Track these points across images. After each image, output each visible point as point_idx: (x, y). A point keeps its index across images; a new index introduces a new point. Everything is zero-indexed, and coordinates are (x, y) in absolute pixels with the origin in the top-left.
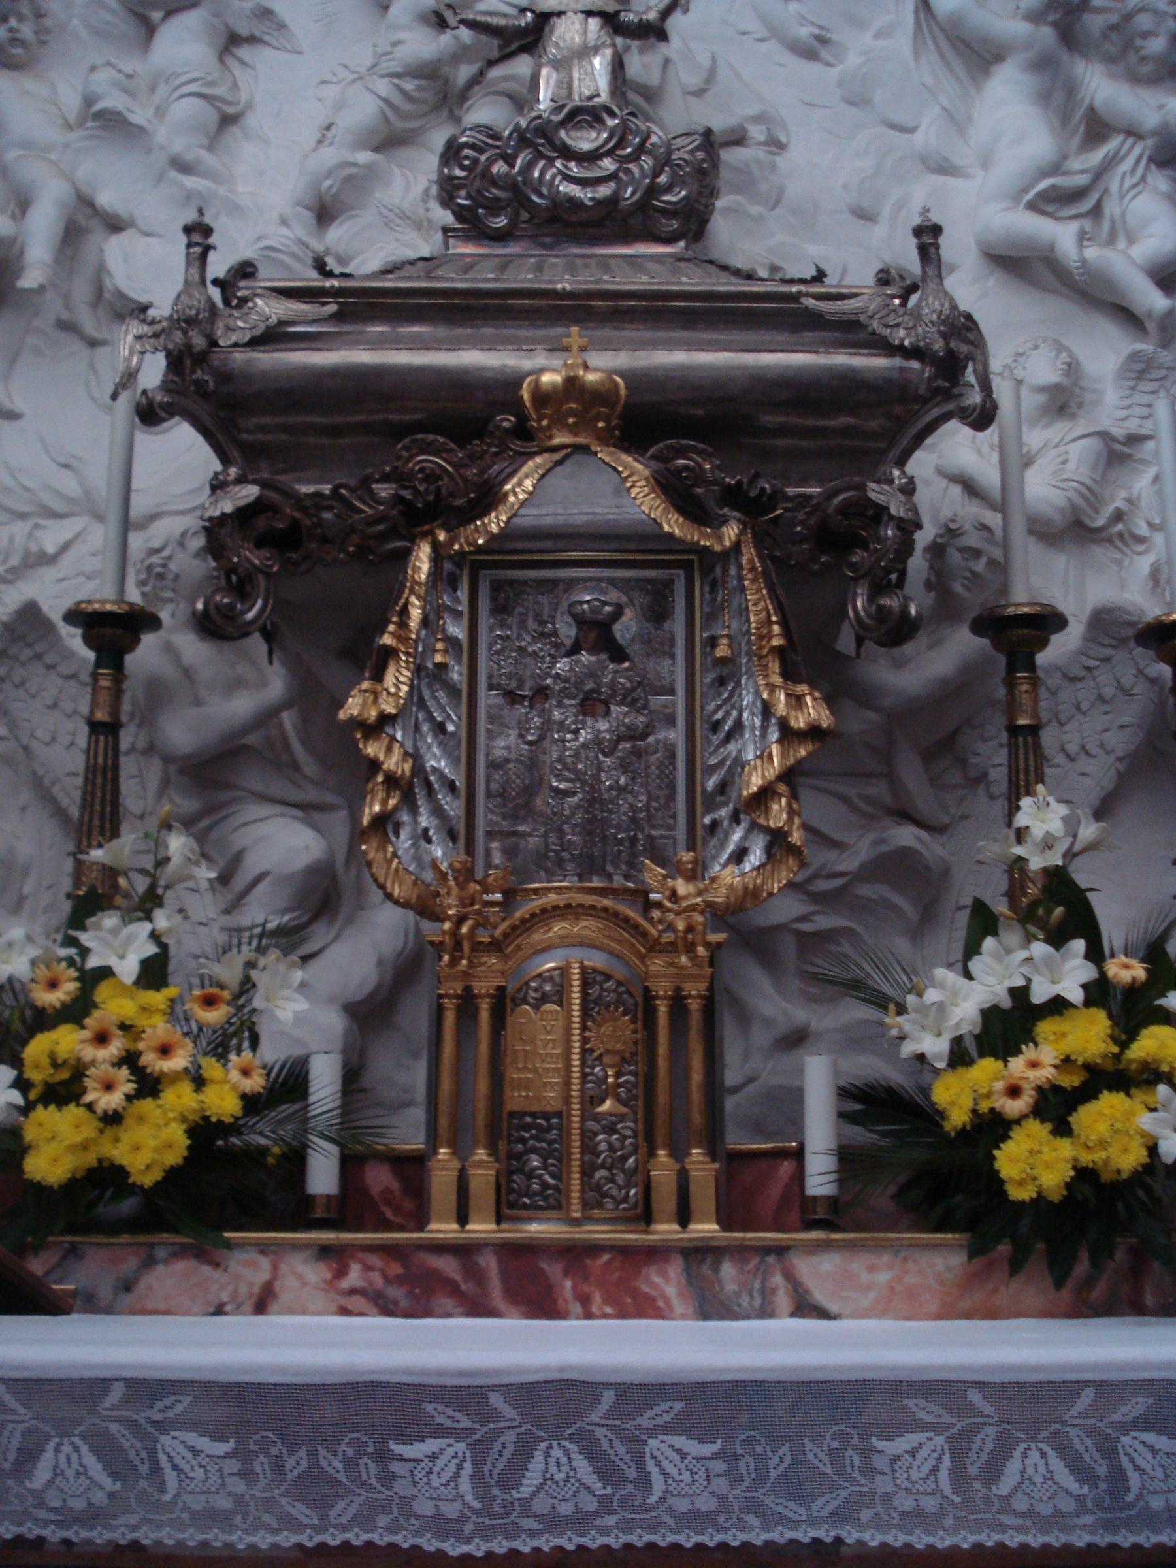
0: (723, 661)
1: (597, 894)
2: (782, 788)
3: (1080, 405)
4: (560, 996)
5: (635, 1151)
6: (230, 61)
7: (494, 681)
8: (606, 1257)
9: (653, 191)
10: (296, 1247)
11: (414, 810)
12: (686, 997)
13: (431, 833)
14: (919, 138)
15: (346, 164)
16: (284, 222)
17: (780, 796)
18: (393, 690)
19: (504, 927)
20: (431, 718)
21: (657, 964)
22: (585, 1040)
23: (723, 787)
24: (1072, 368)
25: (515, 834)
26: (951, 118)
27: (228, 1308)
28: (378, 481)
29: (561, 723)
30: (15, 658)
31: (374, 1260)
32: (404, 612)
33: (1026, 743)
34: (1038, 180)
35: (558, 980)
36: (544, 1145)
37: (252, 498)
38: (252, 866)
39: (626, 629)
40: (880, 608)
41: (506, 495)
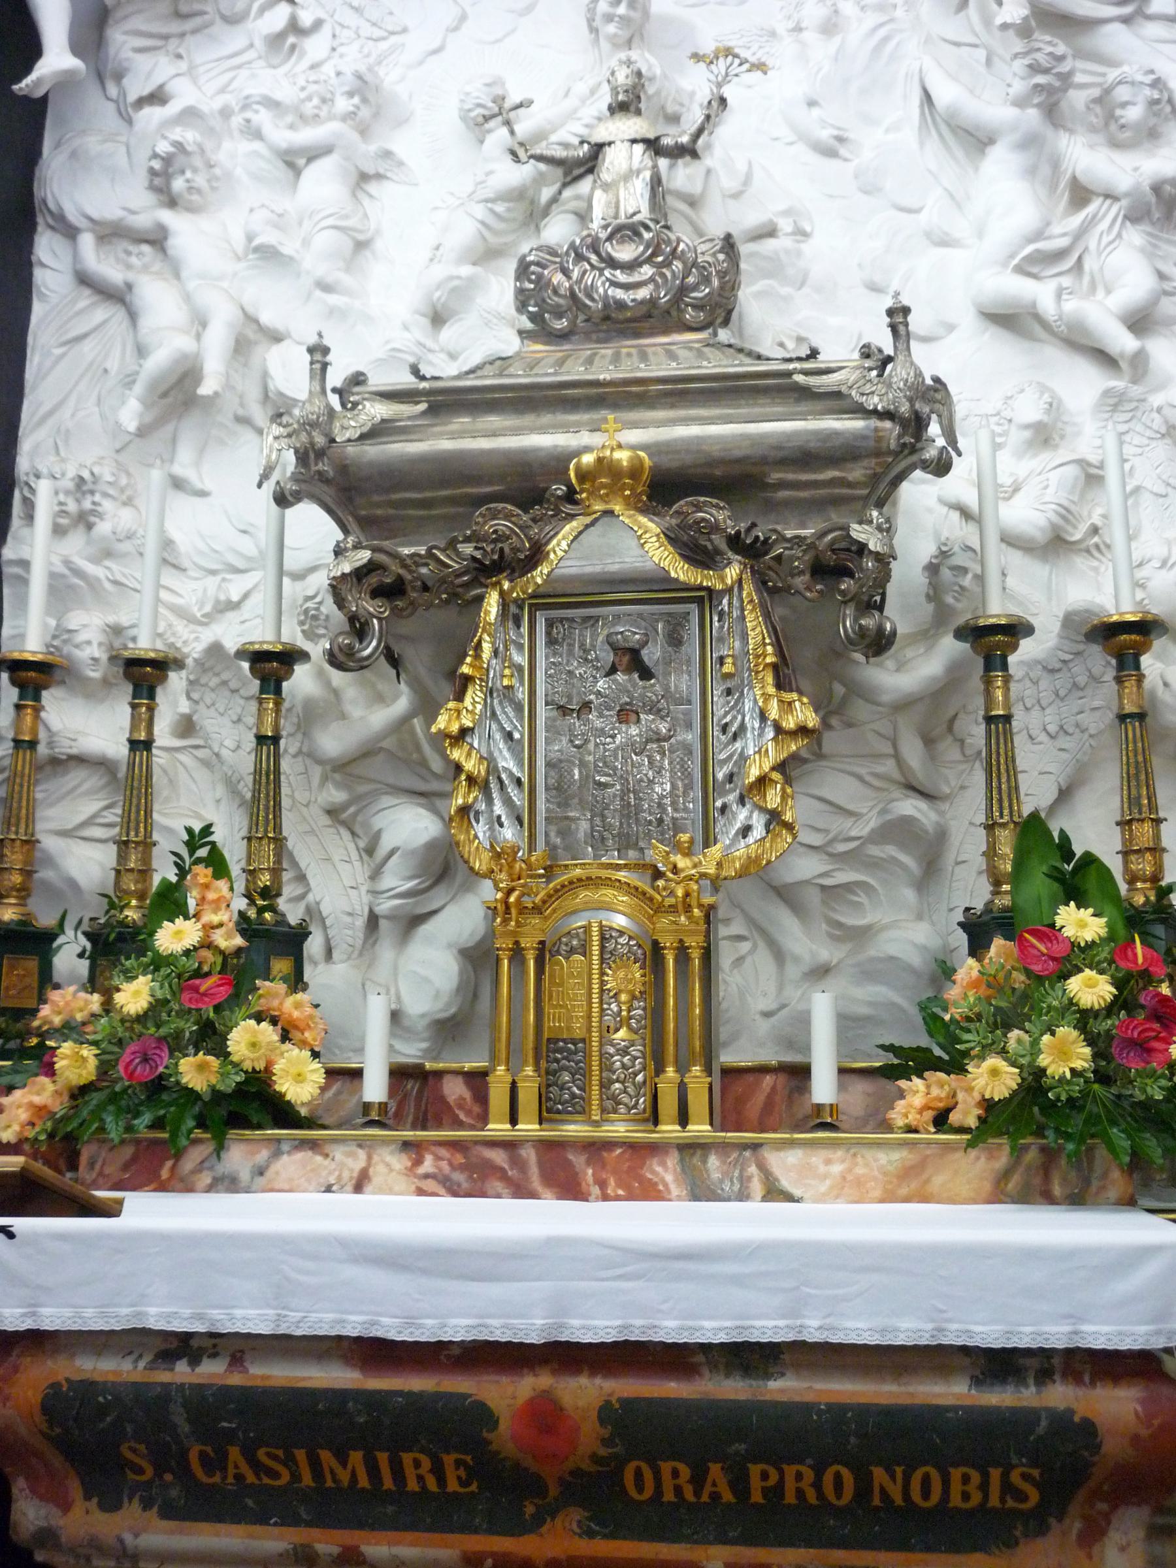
1: (613, 869)
2: (776, 776)
3: (1062, 437)
4: (584, 950)
5: (644, 1069)
6: (361, 195)
7: (549, 699)
8: (619, 1151)
9: (683, 290)
10: (385, 1142)
11: (490, 801)
12: (688, 948)
13: (503, 819)
14: (923, 217)
15: (451, 278)
16: (406, 328)
17: (776, 783)
18: (470, 708)
19: (542, 894)
21: (664, 921)
22: (602, 983)
23: (730, 778)
24: (1054, 406)
25: (567, 818)
26: (952, 196)
27: (334, 1188)
28: (462, 542)
29: (602, 730)
30: (206, 685)
31: (443, 1152)
32: (478, 647)
33: (997, 728)
34: (1022, 247)
35: (582, 936)
36: (572, 1064)
37: (365, 561)
38: (387, 843)
39: (652, 654)
40: (860, 626)
41: (548, 553)
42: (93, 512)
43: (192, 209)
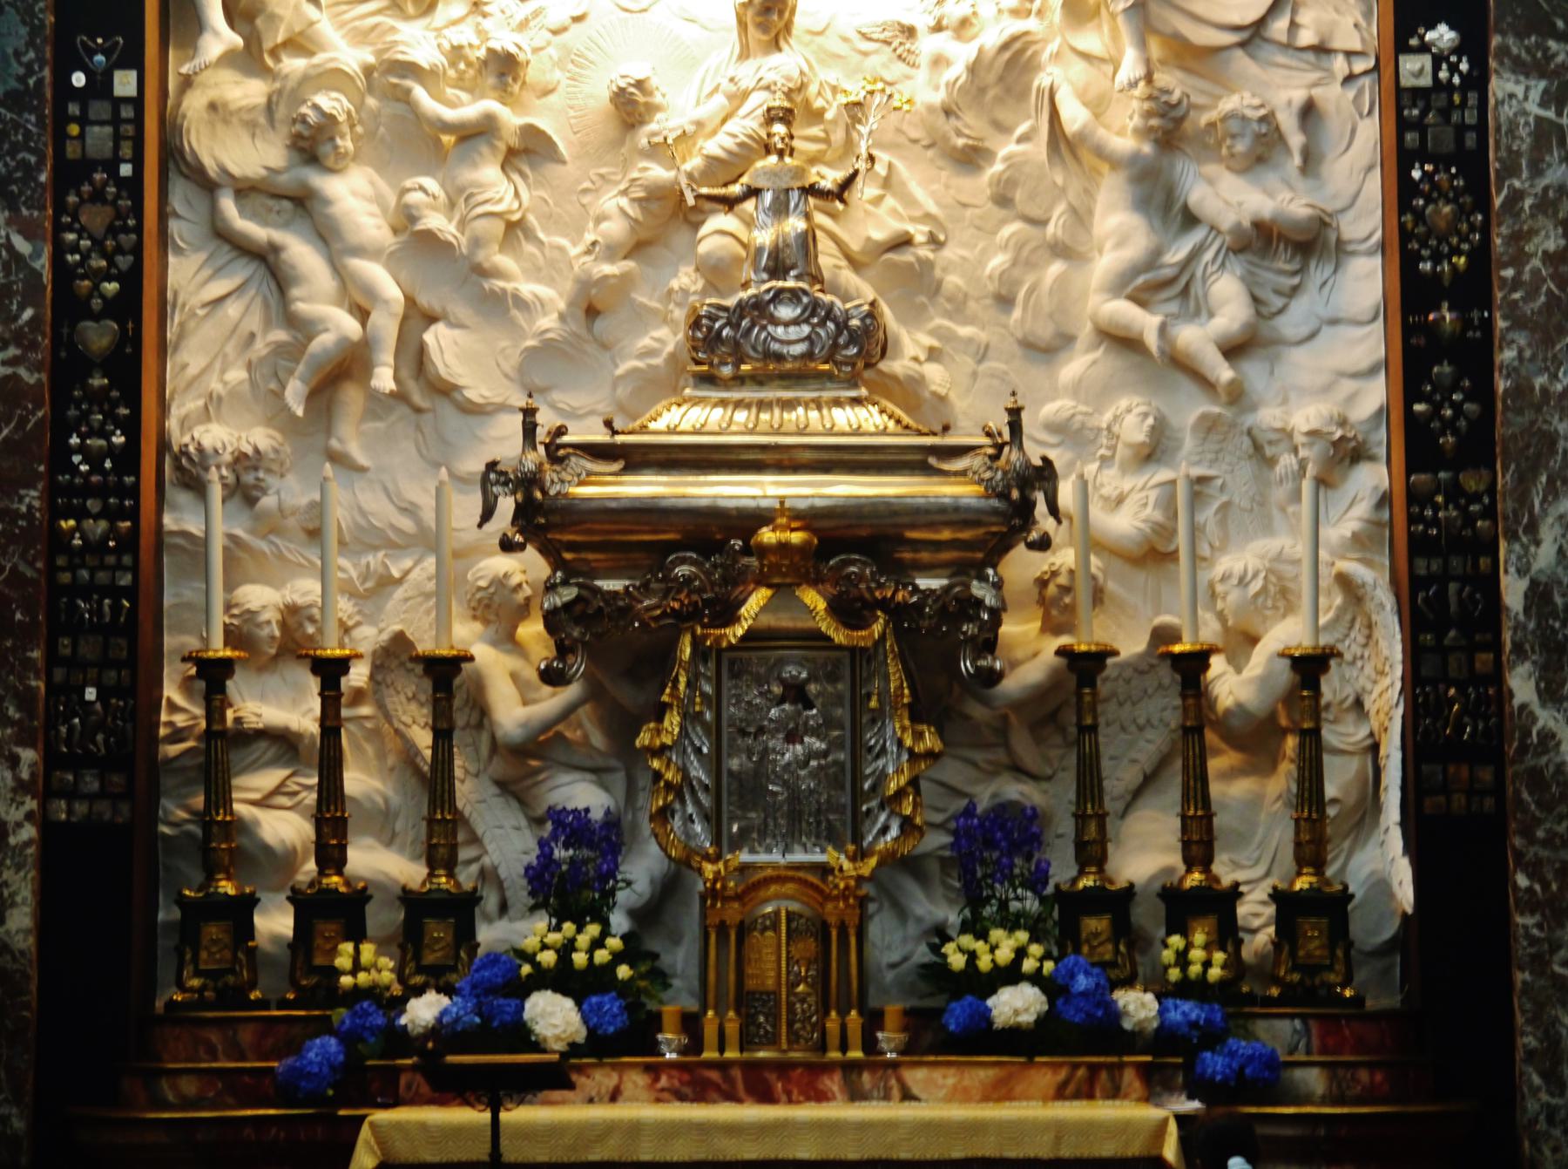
0: (873, 710)
2: (910, 790)
3: (1163, 452)
4: (775, 927)
5: (817, 1012)
8: (799, 1071)
11: (683, 802)
14: (1050, 229)
20: (692, 743)
21: (830, 906)
22: (788, 952)
23: (874, 788)
31: (675, 1073)
32: (676, 681)
42: (256, 487)
43: (332, 171)
